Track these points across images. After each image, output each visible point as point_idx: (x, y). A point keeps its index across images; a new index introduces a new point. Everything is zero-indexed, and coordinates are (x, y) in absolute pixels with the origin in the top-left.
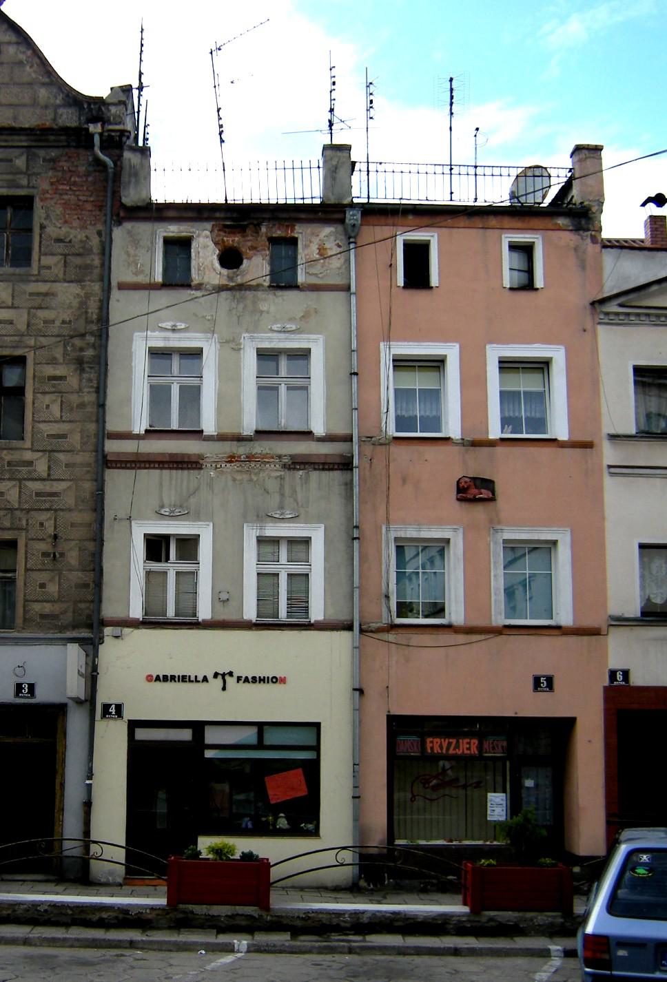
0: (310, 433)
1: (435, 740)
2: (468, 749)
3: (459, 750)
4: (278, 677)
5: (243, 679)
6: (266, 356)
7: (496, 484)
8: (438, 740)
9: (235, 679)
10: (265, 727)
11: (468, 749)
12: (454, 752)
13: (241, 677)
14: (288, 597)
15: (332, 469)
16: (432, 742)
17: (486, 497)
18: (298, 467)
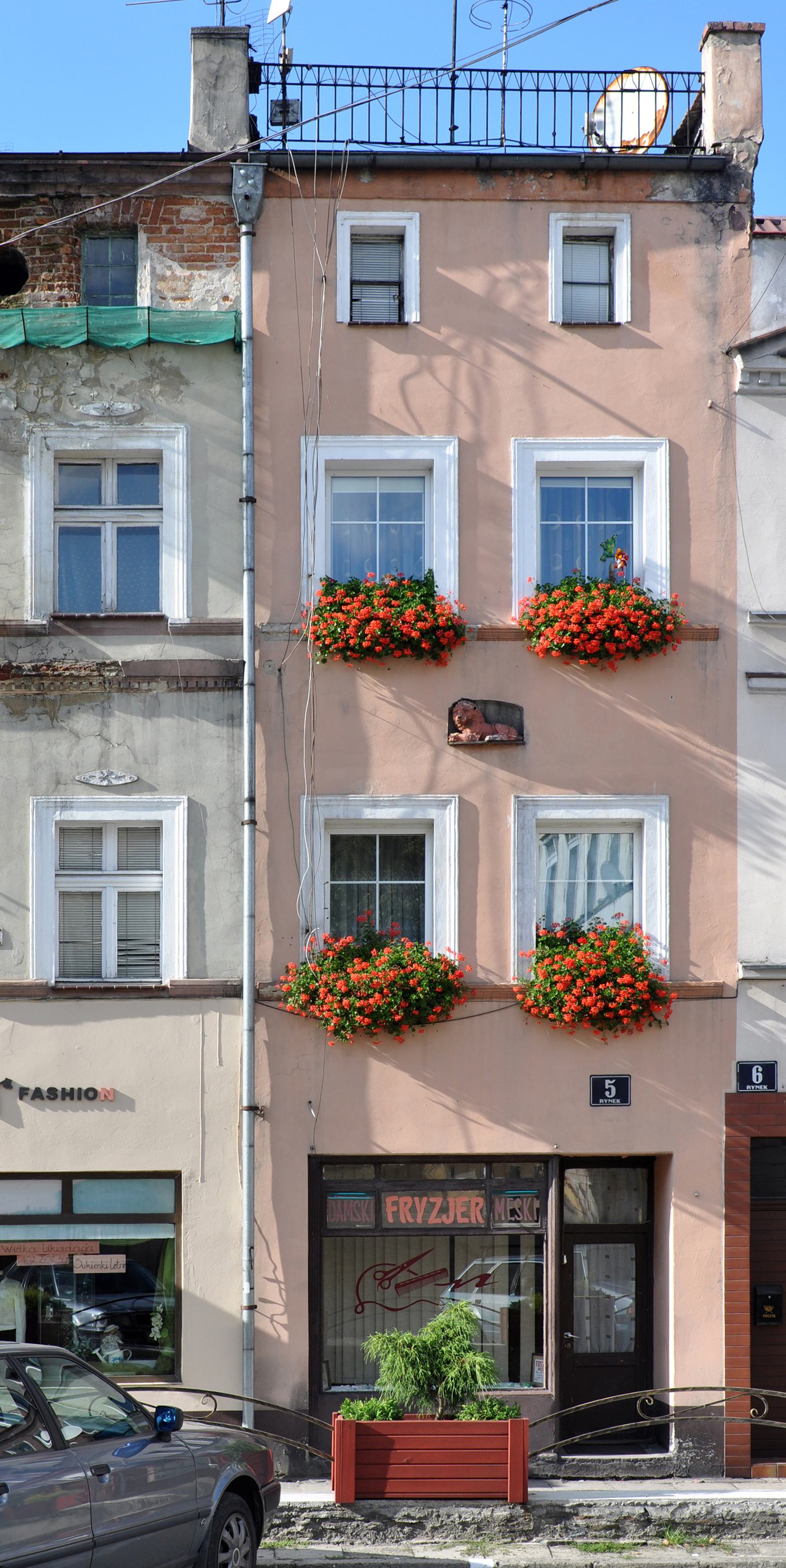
0: (162, 618)
1: (402, 1200)
2: (464, 1215)
3: (448, 1217)
4: (99, 1089)
5: (31, 1093)
6: (77, 475)
7: (525, 712)
8: (409, 1199)
9: (15, 1093)
10: (75, 1182)
11: (464, 1215)
12: (439, 1221)
13: (28, 1089)
14: (118, 936)
15: (204, 689)
16: (396, 1203)
17: (505, 738)
18: (137, 686)
